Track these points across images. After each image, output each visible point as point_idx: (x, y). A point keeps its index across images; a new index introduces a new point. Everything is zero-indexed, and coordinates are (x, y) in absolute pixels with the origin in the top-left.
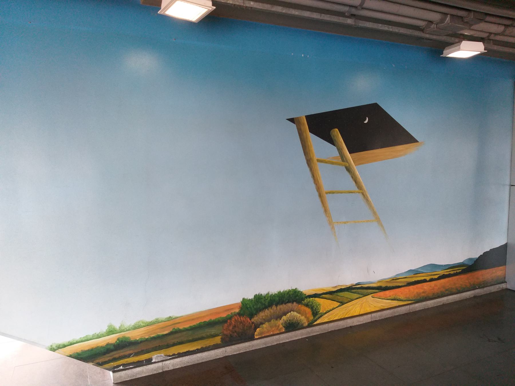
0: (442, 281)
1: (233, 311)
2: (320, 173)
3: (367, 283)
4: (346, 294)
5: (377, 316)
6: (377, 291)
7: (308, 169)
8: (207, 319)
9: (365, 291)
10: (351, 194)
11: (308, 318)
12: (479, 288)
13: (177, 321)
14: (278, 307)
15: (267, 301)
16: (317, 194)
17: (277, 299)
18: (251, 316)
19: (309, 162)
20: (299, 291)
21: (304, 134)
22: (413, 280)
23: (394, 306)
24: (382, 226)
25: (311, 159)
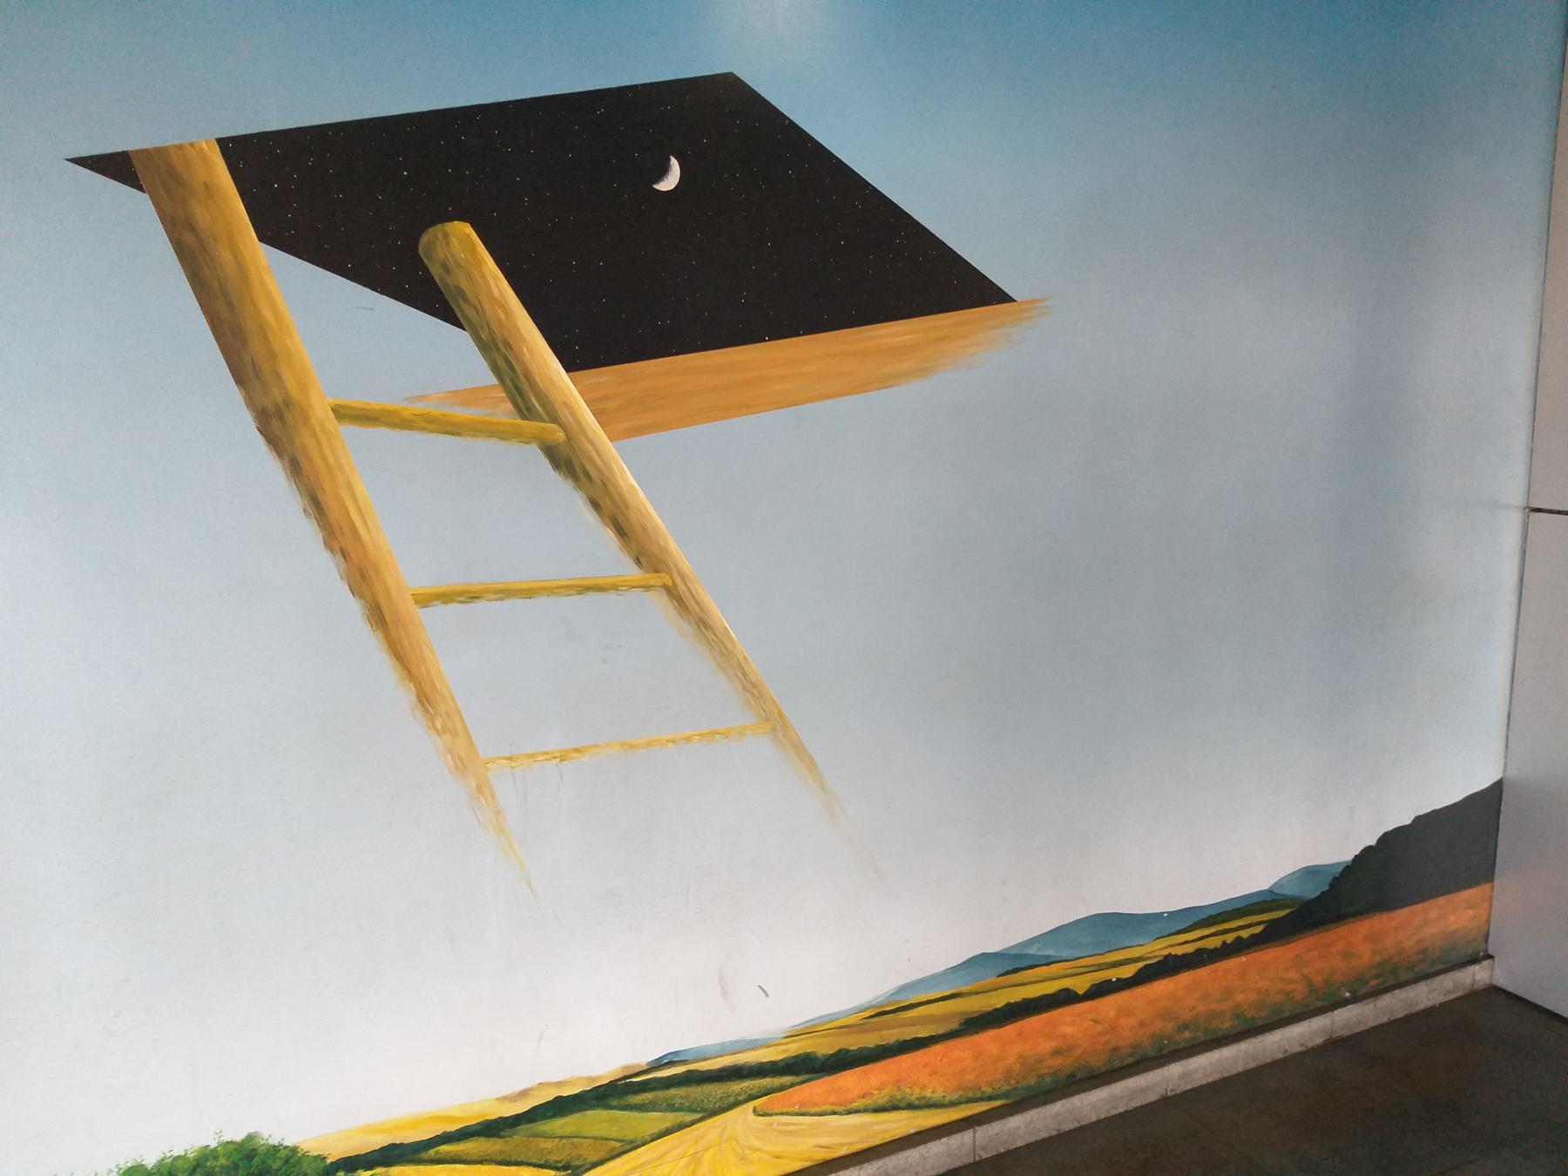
0: (1162, 987)
2: (361, 489)
3: (722, 1051)
4: (597, 1122)
6: (787, 1079)
7: (271, 468)
9: (716, 1090)
12: (1356, 999)
16: (353, 608)
19: (278, 423)
20: (276, 1149)
21: (225, 256)
22: (1002, 997)
23: (888, 1138)
24: (799, 749)
25: (288, 403)
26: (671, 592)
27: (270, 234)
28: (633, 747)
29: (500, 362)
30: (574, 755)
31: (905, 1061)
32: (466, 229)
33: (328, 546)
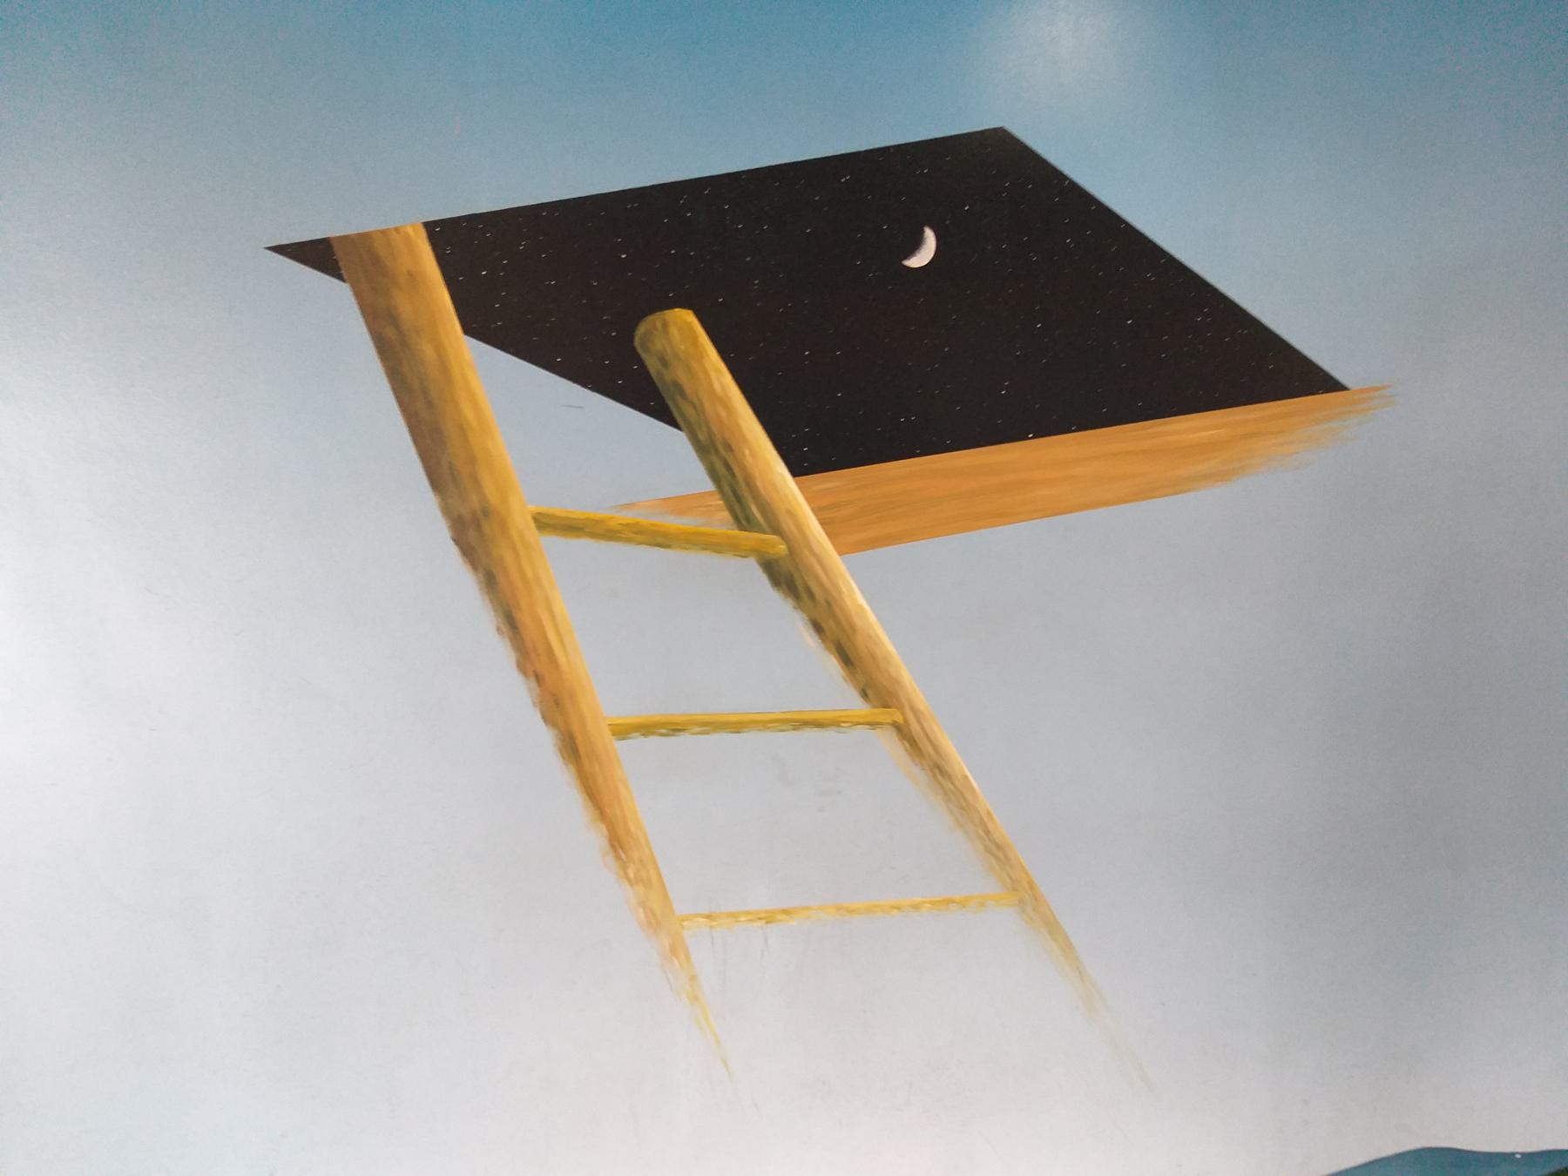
2: (561, 607)
7: (466, 582)
16: (544, 738)
19: (475, 533)
21: (427, 350)
24: (1053, 927)
25: (486, 512)
26: (902, 731)
27: (472, 328)
28: (850, 911)
29: (719, 466)
30: (783, 917)
32: (687, 317)
33: (522, 668)
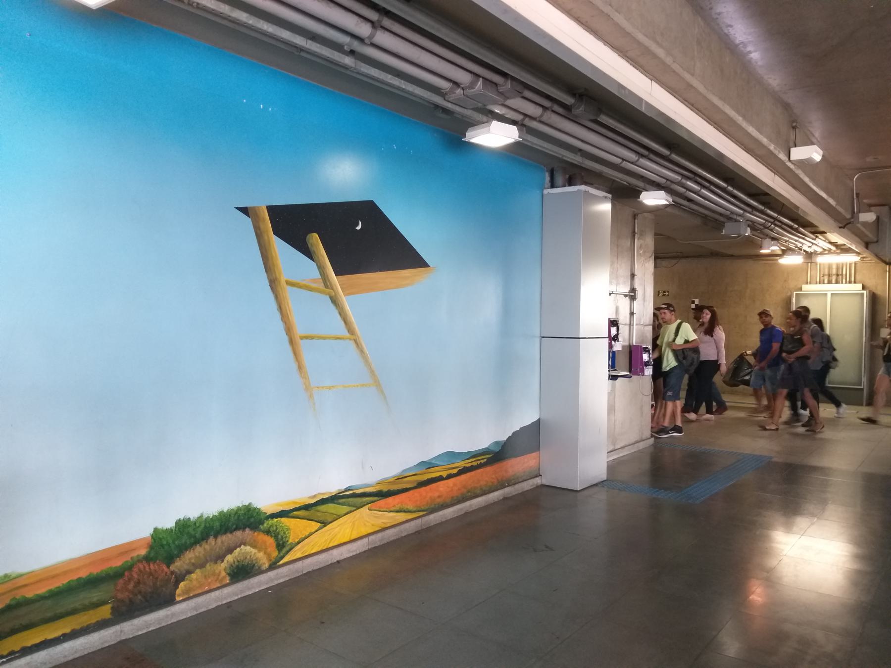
0: (463, 477)
1: (135, 554)
2: (290, 305)
4: (331, 508)
5: (376, 540)
6: (376, 498)
8: (84, 574)
10: (338, 341)
11: (268, 555)
12: (509, 486)
13: (21, 582)
14: (219, 540)
15: (200, 529)
16: (286, 338)
17: (217, 524)
18: (170, 559)
19: (274, 283)
20: (255, 508)
21: (266, 238)
26: (355, 341)
27: (276, 233)
31: (404, 495)
32: (316, 235)
